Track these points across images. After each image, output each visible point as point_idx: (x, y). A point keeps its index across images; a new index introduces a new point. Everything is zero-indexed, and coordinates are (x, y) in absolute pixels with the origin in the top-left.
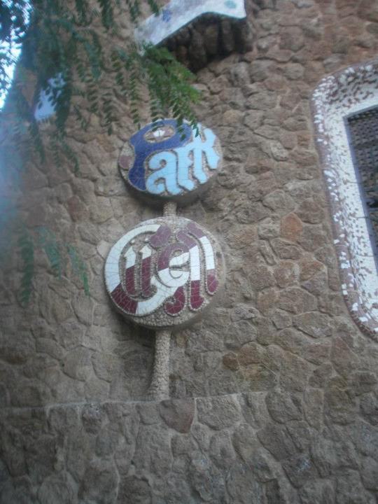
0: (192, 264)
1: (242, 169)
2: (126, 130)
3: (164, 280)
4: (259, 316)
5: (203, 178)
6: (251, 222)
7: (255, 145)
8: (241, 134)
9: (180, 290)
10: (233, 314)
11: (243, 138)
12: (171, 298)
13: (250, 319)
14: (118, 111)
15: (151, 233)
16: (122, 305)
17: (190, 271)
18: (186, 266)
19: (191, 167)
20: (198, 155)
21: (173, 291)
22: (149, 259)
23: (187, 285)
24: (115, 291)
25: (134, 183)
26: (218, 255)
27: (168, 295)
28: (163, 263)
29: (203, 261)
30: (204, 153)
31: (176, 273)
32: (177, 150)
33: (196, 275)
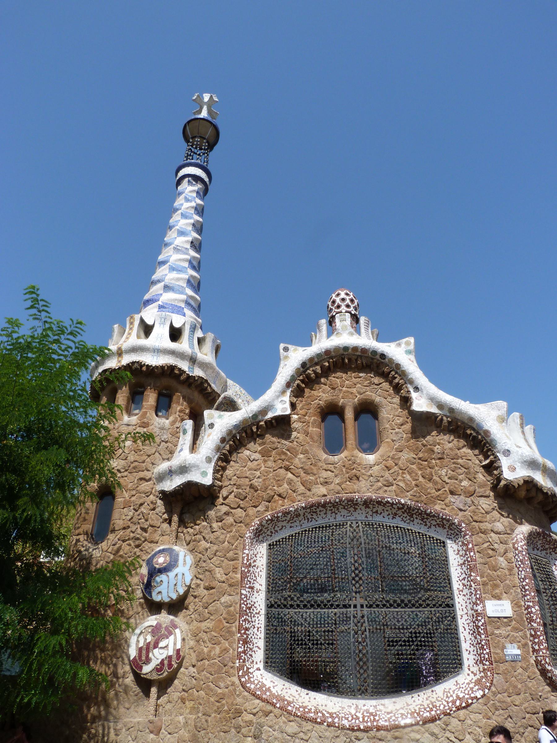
0: (169, 646)
1: (202, 586)
2: (145, 552)
3: (156, 655)
4: (198, 676)
5: (181, 591)
6: (201, 621)
7: (210, 571)
8: (204, 562)
9: (163, 660)
10: (187, 673)
11: (204, 565)
12: (158, 665)
13: (193, 677)
14: (141, 540)
15: (152, 626)
16: (136, 667)
17: (168, 650)
18: (166, 647)
19: (175, 585)
20: (180, 576)
21: (160, 660)
22: (149, 643)
23: (166, 658)
24: (133, 659)
25: (147, 593)
26: (183, 640)
27: (157, 663)
28: (156, 646)
29: (175, 644)
30: (183, 574)
31: (161, 651)
32: (169, 574)
33: (171, 652)
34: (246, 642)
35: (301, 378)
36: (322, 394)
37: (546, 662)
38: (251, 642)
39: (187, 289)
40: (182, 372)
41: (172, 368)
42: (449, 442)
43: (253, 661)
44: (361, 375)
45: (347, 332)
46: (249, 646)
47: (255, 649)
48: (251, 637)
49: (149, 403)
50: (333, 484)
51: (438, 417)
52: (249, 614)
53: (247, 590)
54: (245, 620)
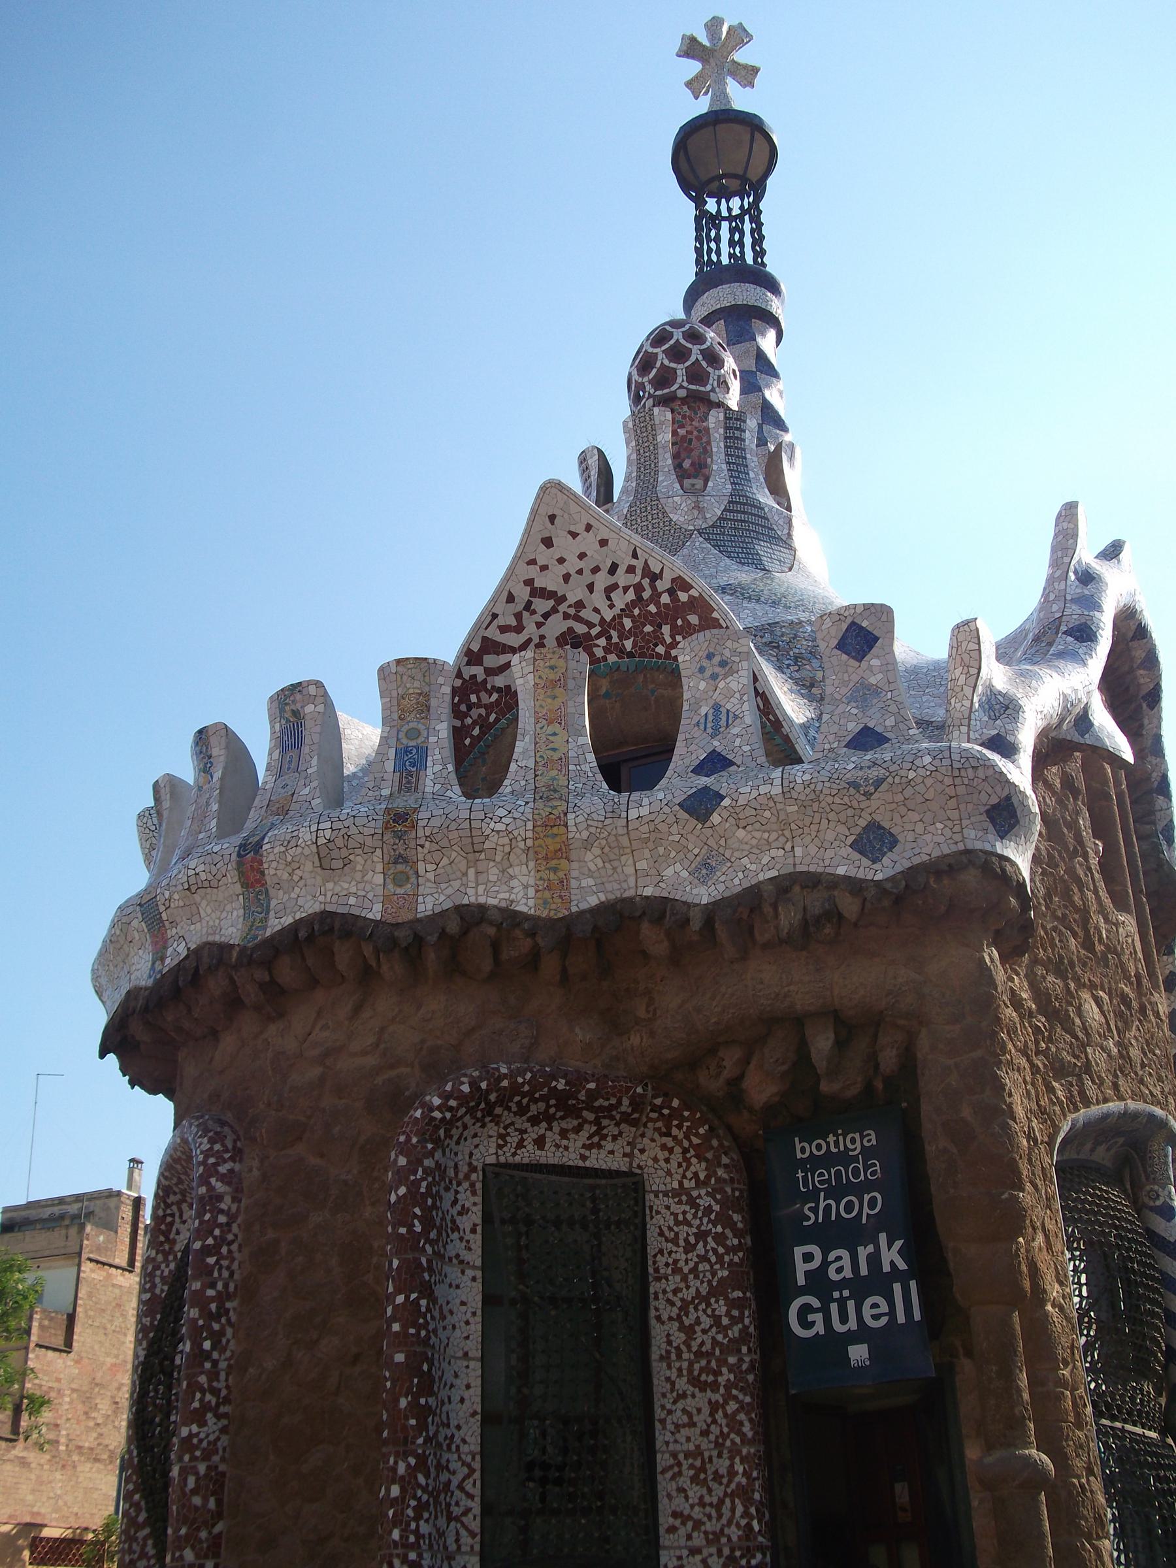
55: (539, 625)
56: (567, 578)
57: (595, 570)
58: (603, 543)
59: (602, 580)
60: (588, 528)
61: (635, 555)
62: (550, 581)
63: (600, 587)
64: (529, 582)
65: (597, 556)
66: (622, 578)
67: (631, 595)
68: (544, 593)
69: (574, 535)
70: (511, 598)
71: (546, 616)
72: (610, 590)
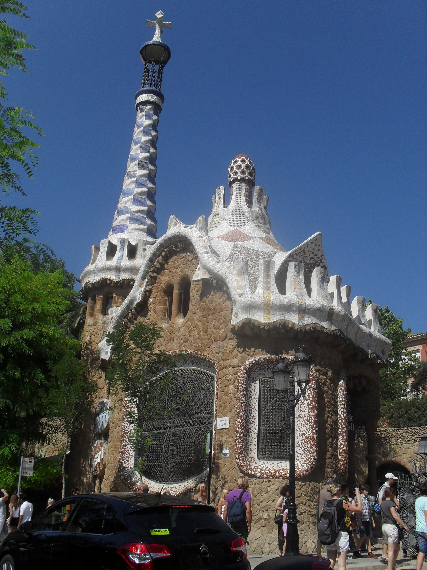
26: (105, 453)
29: (101, 456)
34: (123, 453)
35: (152, 269)
36: (163, 279)
37: (236, 458)
38: (127, 452)
39: (147, 200)
40: (111, 280)
41: (105, 280)
42: (220, 299)
43: (129, 464)
44: (184, 255)
45: (173, 223)
46: (126, 455)
47: (131, 457)
48: (128, 450)
49: (97, 308)
50: (162, 347)
51: (210, 280)
52: (127, 437)
53: (125, 422)
54: (123, 441)
55: (299, 257)
56: (309, 251)
57: (313, 253)
58: (319, 250)
59: (312, 255)
60: (319, 246)
61: (321, 256)
62: (306, 250)
63: (311, 256)
64: (305, 248)
65: (316, 252)
66: (315, 258)
67: (314, 262)
68: (304, 251)
69: (316, 245)
70: (300, 249)
71: (301, 256)
72: (312, 258)
